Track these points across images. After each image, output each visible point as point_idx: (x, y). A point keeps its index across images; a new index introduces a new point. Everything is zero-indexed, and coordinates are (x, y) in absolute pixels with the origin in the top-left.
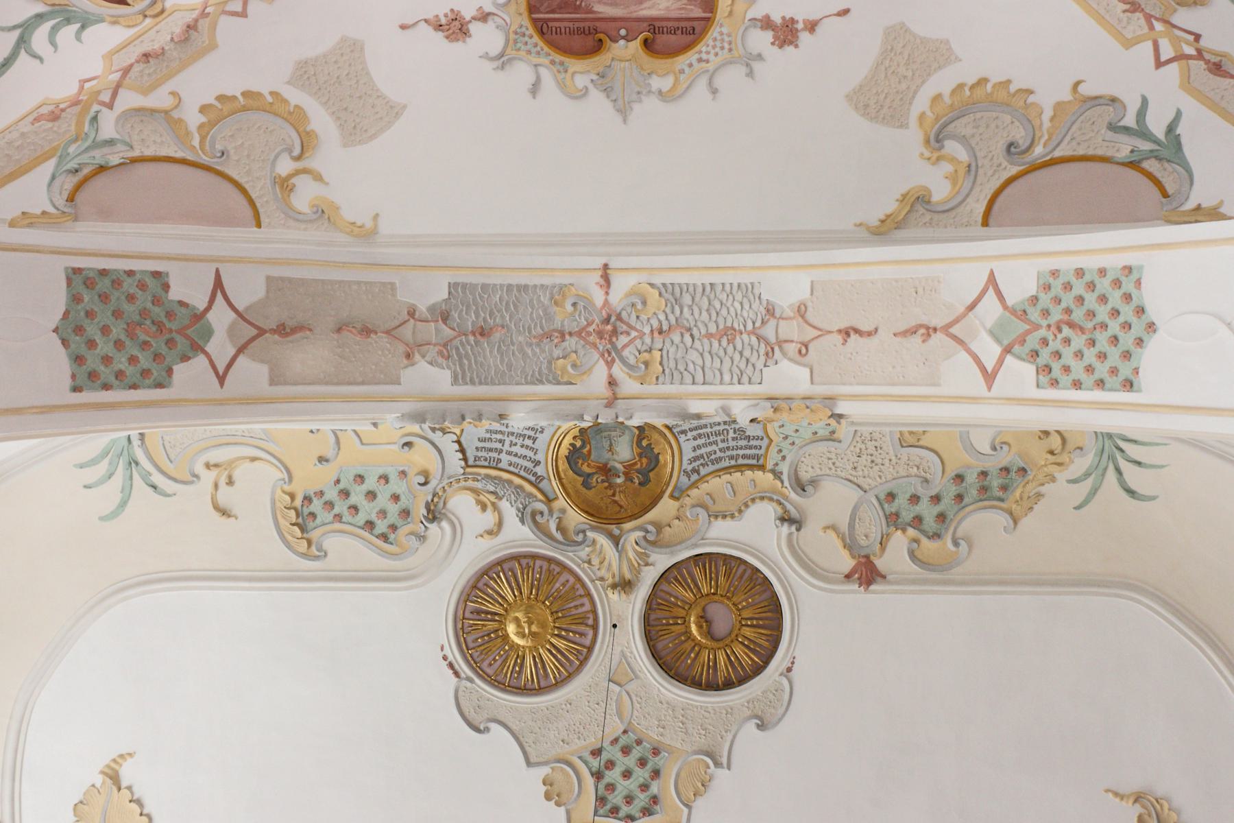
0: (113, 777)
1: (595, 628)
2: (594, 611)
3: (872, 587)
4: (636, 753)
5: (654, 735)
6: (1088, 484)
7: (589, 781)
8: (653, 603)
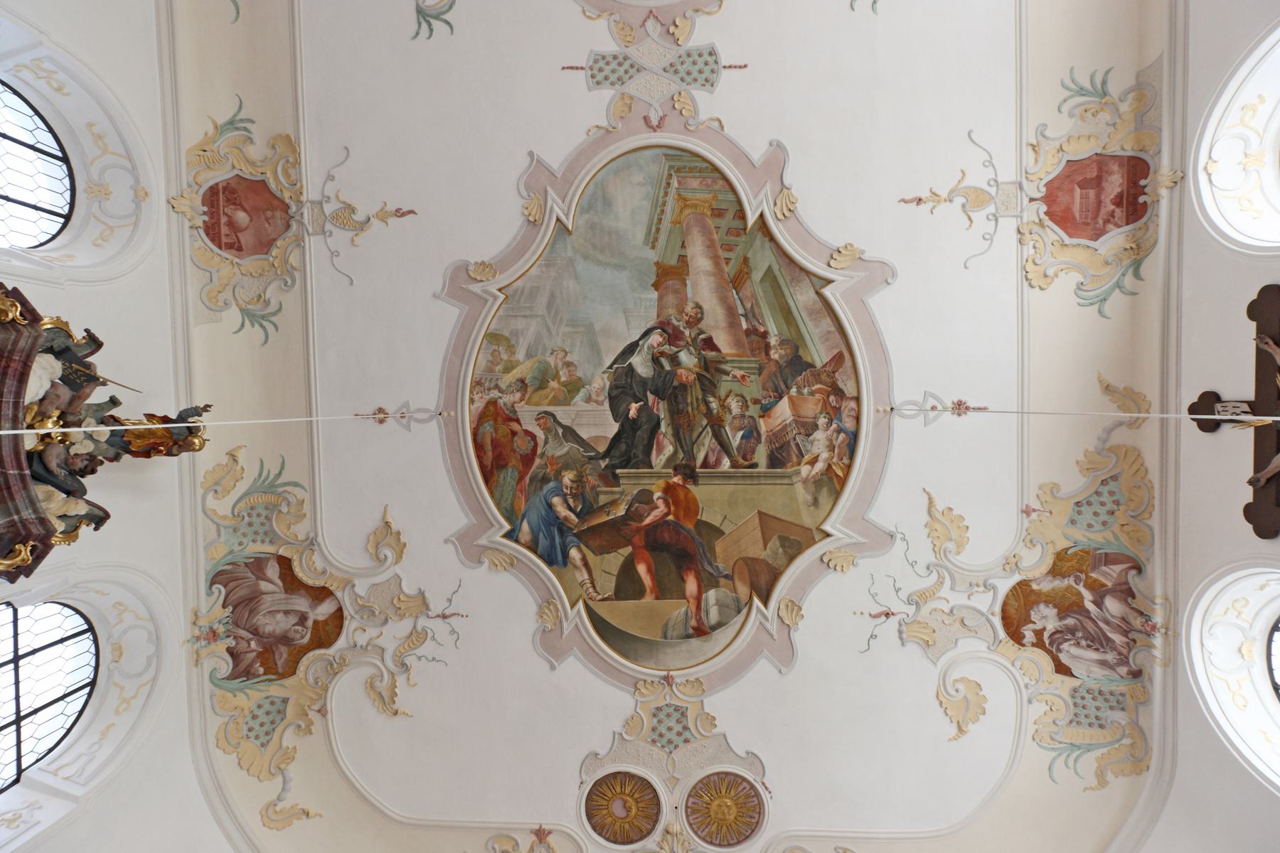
0: (960, 729)
1: (687, 807)
2: (687, 816)
3: (537, 827)
4: (664, 741)
5: (656, 750)
7: (691, 725)
8: (654, 817)
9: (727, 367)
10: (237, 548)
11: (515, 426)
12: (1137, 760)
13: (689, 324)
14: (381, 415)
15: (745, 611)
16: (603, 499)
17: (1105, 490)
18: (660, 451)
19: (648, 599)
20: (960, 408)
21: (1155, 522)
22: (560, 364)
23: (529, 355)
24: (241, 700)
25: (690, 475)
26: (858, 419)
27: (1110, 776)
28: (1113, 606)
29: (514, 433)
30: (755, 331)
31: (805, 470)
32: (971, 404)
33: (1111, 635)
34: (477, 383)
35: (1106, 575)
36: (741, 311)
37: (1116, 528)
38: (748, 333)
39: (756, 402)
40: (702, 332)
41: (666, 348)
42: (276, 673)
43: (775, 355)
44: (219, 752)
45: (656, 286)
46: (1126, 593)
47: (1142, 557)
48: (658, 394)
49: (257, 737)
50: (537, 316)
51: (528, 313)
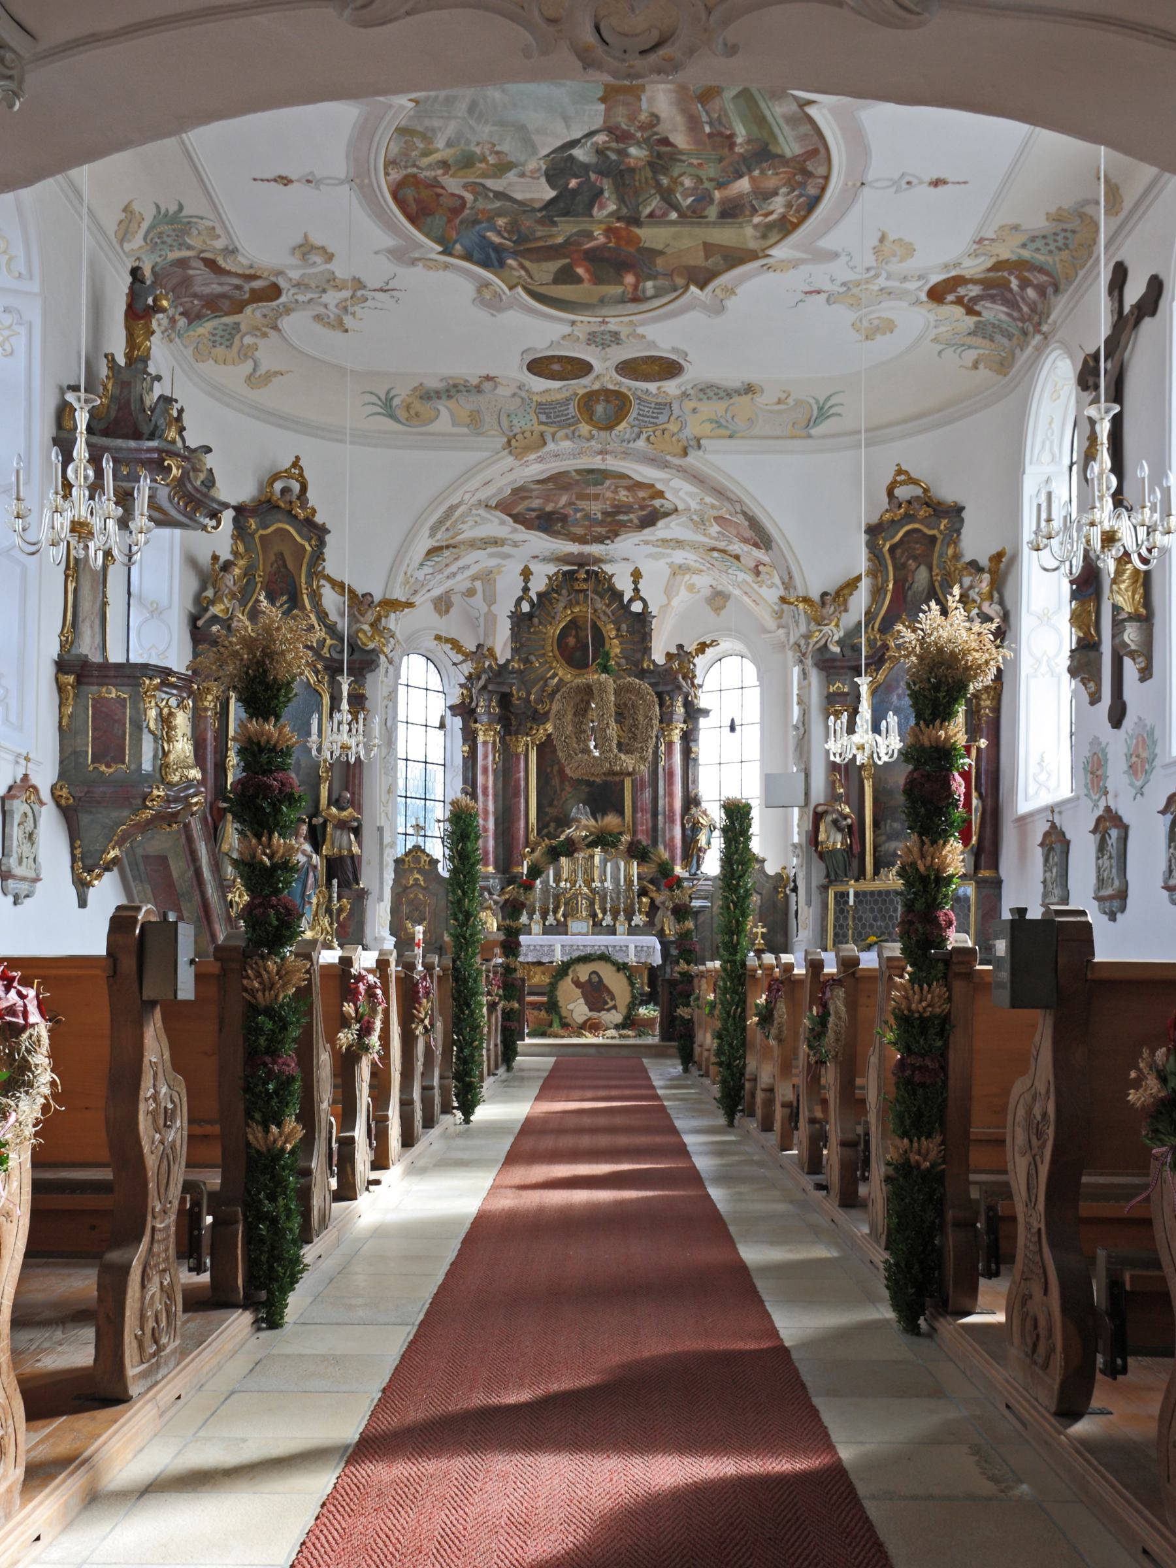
6: (392, 394)
9: (684, 158)
10: (159, 260)
11: (440, 191)
12: (1003, 366)
13: (642, 128)
14: (285, 181)
15: (680, 291)
16: (539, 234)
17: (1062, 234)
18: (602, 207)
19: (586, 285)
20: (936, 183)
21: (1081, 273)
22: (487, 153)
23: (449, 144)
24: (201, 330)
25: (635, 221)
26: (823, 189)
27: (981, 366)
28: (1031, 293)
29: (438, 195)
30: (721, 134)
31: (757, 220)
32: (950, 179)
33: (1022, 305)
34: (390, 163)
35: (1036, 277)
36: (705, 118)
37: (1057, 259)
38: (710, 135)
39: (711, 180)
40: (656, 134)
41: (614, 145)
42: (222, 310)
43: (738, 149)
44: (200, 364)
45: (603, 100)
46: (1041, 291)
47: (1062, 287)
48: (601, 173)
49: (221, 344)
50: (456, 118)
51: (446, 114)
